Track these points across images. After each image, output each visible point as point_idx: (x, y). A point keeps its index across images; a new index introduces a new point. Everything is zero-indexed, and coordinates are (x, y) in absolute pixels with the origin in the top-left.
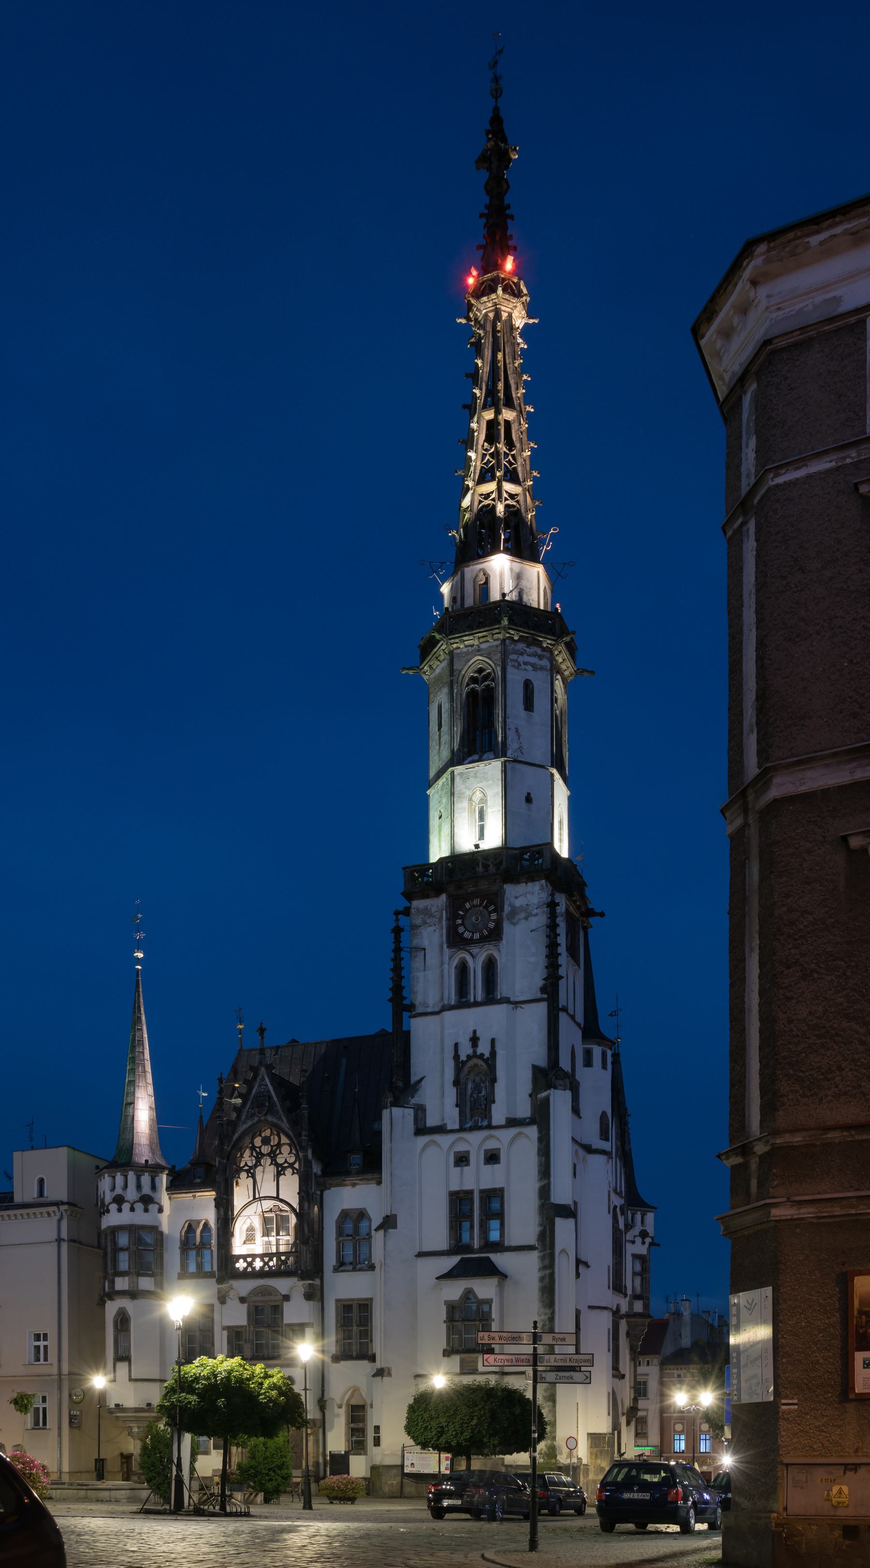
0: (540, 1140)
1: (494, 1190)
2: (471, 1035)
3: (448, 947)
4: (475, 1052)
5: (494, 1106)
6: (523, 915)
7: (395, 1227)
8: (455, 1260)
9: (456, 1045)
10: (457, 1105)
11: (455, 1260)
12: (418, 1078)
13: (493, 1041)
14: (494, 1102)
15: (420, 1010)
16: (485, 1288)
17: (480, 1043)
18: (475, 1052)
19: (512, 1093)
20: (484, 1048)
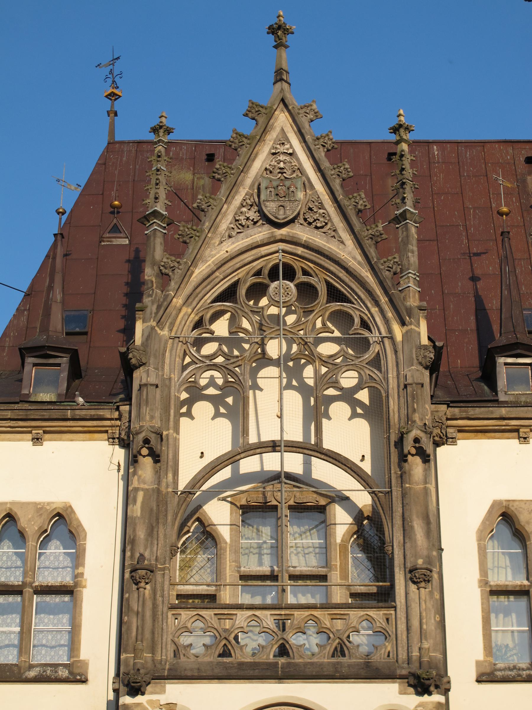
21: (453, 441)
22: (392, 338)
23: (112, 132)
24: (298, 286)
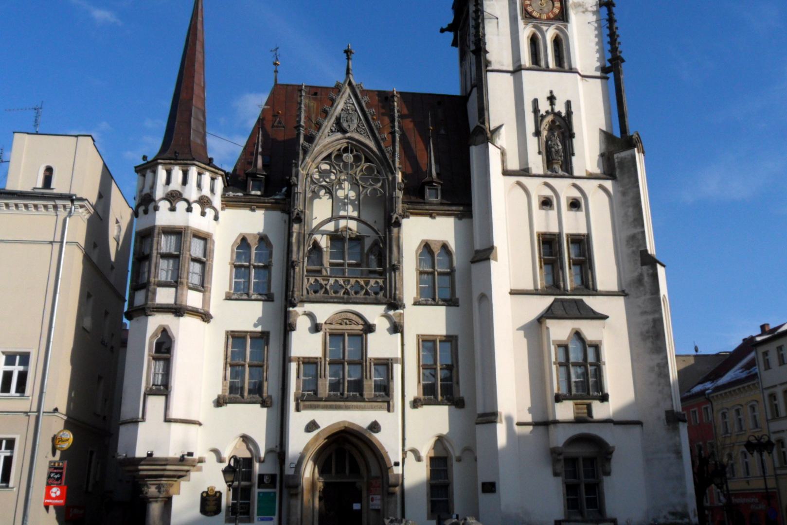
0: (624, 194)
1: (579, 235)
2: (549, 95)
3: (523, 19)
4: (552, 109)
5: (574, 159)
6: (581, 9)
7: (496, 260)
8: (549, 300)
9: (535, 102)
10: (540, 153)
11: (549, 300)
12: (497, 125)
13: (568, 104)
14: (573, 154)
15: (494, 66)
16: (590, 330)
17: (557, 102)
18: (552, 109)
19: (587, 152)
20: (560, 107)
21: (408, 217)
22: (388, 179)
23: (276, 80)
24: (354, 156)
